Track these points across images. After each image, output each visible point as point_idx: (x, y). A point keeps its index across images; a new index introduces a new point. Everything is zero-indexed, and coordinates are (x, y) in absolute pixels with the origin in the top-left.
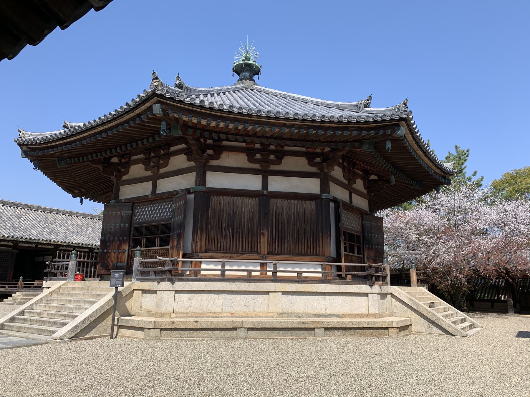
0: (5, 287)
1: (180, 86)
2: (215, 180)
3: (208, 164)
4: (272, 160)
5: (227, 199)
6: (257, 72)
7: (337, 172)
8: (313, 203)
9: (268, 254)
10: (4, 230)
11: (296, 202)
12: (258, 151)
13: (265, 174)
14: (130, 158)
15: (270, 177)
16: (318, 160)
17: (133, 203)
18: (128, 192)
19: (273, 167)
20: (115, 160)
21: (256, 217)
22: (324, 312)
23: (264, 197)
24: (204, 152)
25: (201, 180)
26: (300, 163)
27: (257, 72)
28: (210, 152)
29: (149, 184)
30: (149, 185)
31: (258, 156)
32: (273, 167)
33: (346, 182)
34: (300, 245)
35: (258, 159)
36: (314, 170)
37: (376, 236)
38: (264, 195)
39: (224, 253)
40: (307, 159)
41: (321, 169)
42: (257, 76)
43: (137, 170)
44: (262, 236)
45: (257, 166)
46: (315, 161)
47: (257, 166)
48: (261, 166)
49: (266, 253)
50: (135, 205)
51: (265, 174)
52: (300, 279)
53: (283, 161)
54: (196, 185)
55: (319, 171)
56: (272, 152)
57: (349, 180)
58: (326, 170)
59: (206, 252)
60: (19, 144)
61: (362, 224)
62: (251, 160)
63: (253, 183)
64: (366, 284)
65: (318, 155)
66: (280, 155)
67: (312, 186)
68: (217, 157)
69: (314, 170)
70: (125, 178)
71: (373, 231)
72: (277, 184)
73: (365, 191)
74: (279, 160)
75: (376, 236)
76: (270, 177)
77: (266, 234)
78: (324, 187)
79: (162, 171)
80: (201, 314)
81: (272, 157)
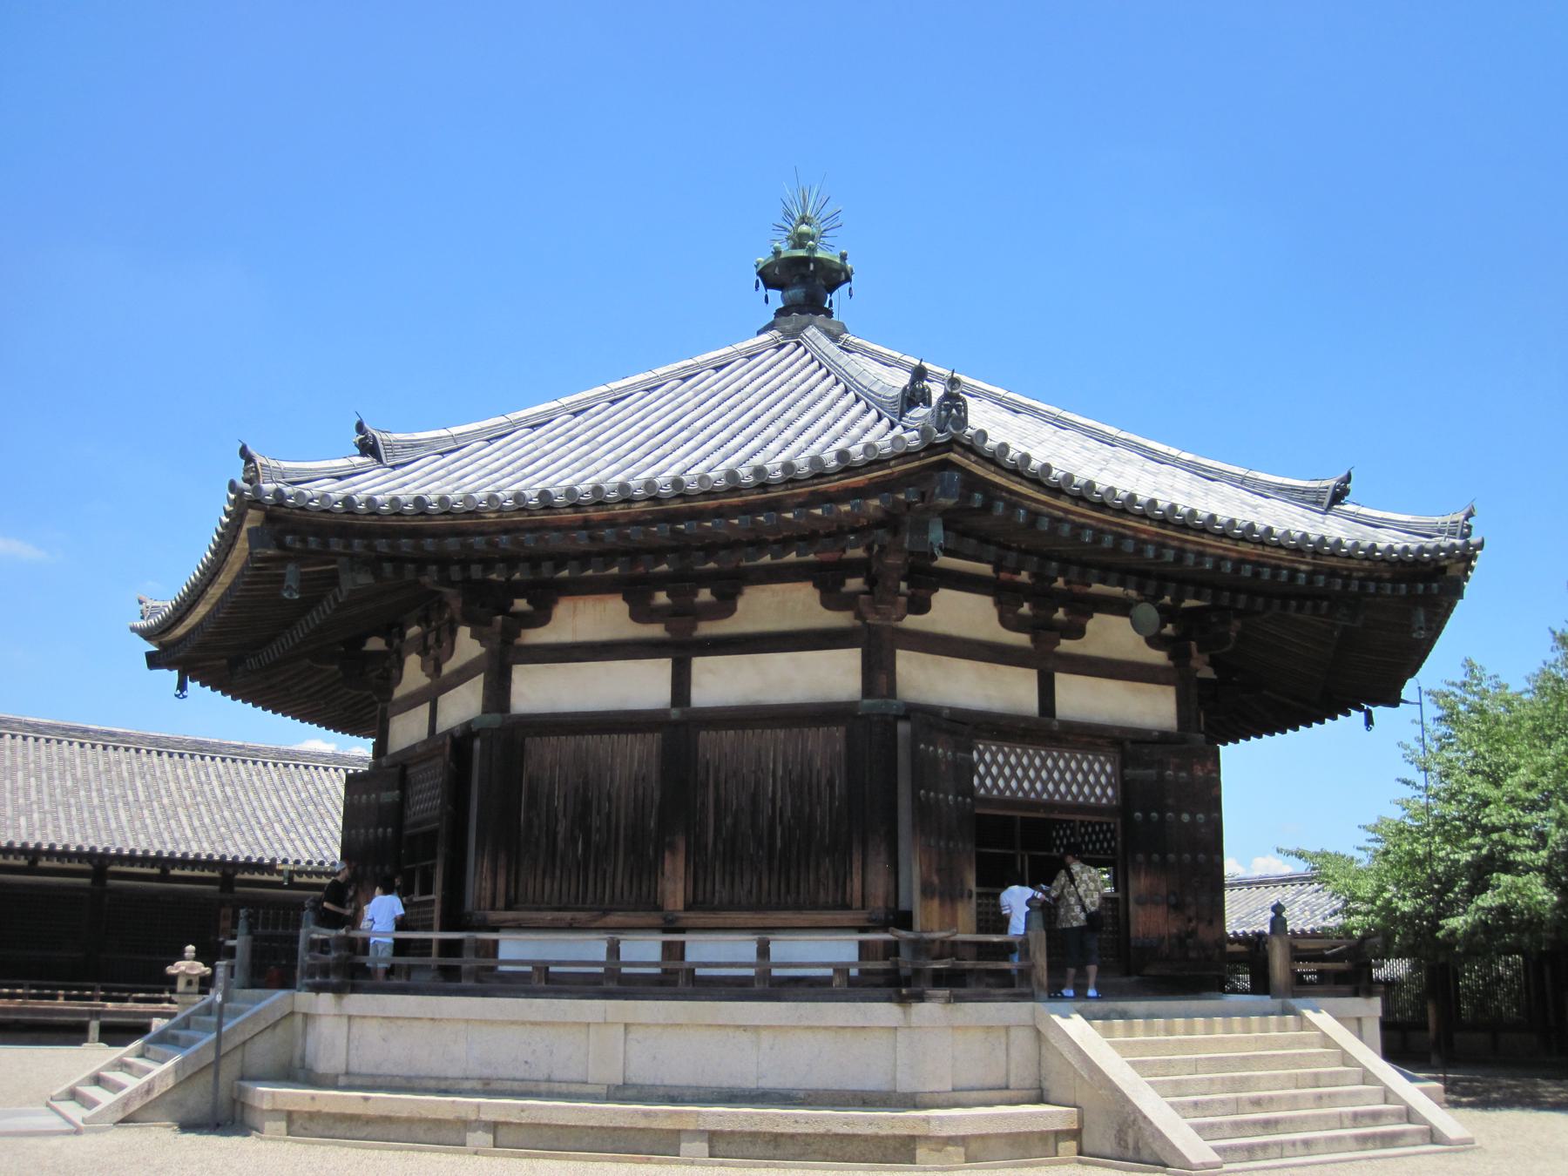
0: (55, 997)
1: (368, 448)
2: (539, 690)
3: (518, 641)
4: (706, 605)
5: (569, 743)
6: (835, 276)
7: (961, 612)
8: (839, 732)
9: (688, 908)
10: (309, 844)
11: (781, 734)
12: (661, 582)
13: (681, 652)
14: (402, 635)
15: (700, 665)
16: (854, 584)
17: (404, 768)
18: (408, 730)
19: (707, 629)
20: (375, 644)
21: (657, 795)
22: (750, 1083)
23: (679, 727)
24: (504, 609)
25: (498, 693)
26: (796, 604)
27: (835, 276)
28: (521, 604)
29: (425, 709)
30: (424, 711)
31: (662, 598)
32: (707, 629)
33: (1022, 639)
34: (793, 874)
35: (663, 608)
36: (839, 619)
37: (1186, 817)
38: (676, 724)
39: (559, 910)
40: (815, 586)
41: (859, 615)
42: (844, 289)
43: (414, 674)
44: (667, 854)
45: (656, 631)
46: (844, 590)
47: (656, 631)
48: (667, 629)
49: (680, 906)
50: (410, 771)
51: (681, 652)
52: (769, 986)
53: (741, 603)
54: (484, 712)
55: (858, 623)
56: (704, 579)
57: (1041, 629)
58: (873, 620)
59: (508, 907)
60: (147, 634)
61: (1122, 776)
62: (640, 613)
63: (642, 685)
64: (889, 1000)
65: (854, 568)
66: (729, 590)
67: (834, 675)
68: (541, 617)
69: (839, 619)
70: (399, 692)
71: (1170, 801)
72: (721, 682)
73: (1158, 657)
74: (725, 605)
75: (1186, 817)
76: (700, 665)
77: (681, 845)
78: (877, 671)
79: (447, 668)
80: (409, 1078)
81: (705, 595)
